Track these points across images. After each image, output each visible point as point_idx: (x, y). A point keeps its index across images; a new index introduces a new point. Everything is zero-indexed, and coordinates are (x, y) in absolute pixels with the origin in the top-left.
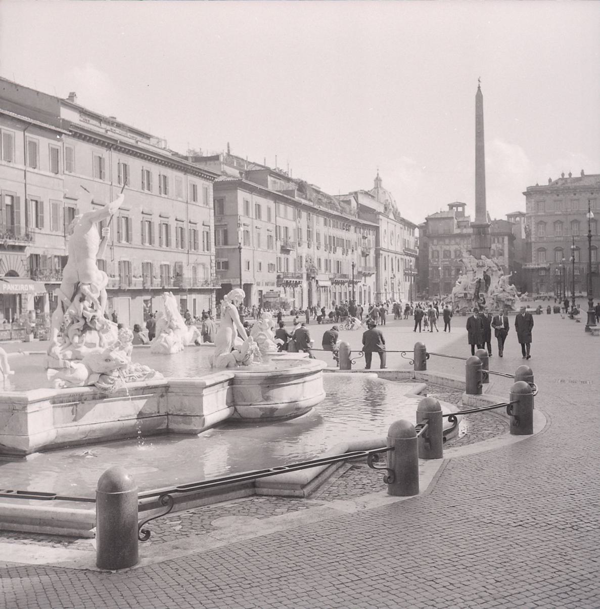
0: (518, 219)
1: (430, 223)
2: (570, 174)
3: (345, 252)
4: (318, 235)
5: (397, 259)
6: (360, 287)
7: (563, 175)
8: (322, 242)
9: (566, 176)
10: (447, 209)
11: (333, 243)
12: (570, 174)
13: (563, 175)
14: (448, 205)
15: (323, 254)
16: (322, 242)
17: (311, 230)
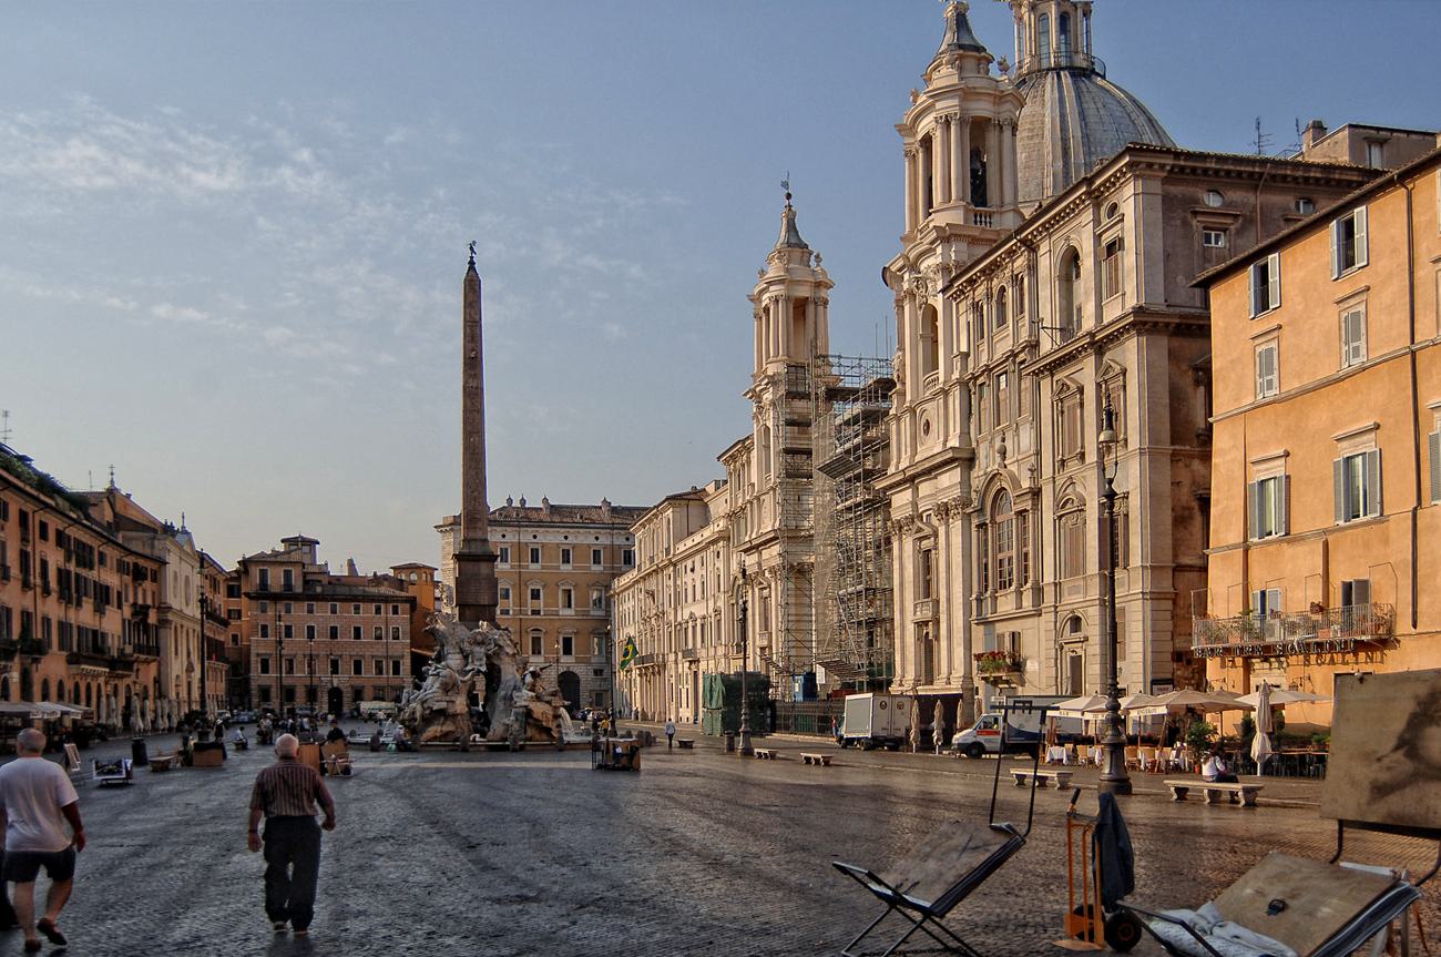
0: (414, 577)
1: (255, 571)
2: (523, 501)
3: (99, 610)
4: (44, 564)
5: (185, 629)
6: (128, 686)
7: (510, 501)
8: (53, 584)
9: (516, 504)
10: (281, 548)
11: (70, 590)
12: (523, 501)
13: (510, 501)
14: (283, 541)
15: (52, 608)
16: (53, 584)
17: (29, 549)
